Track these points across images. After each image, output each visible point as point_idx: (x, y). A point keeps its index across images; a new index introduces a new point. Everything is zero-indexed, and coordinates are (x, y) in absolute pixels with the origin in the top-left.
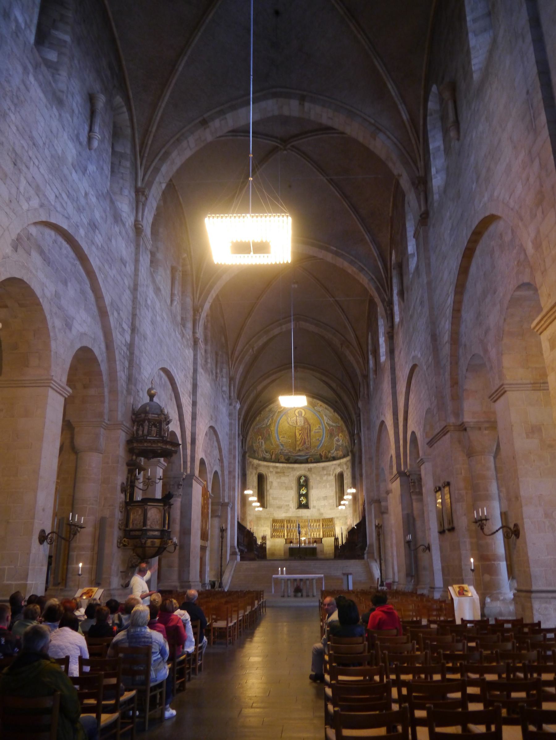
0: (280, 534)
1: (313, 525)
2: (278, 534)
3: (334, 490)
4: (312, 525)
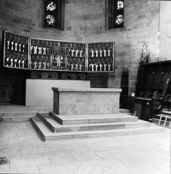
0: (20, 61)
1: (74, 53)
2: (16, 60)
3: (104, 7)
4: (73, 51)
